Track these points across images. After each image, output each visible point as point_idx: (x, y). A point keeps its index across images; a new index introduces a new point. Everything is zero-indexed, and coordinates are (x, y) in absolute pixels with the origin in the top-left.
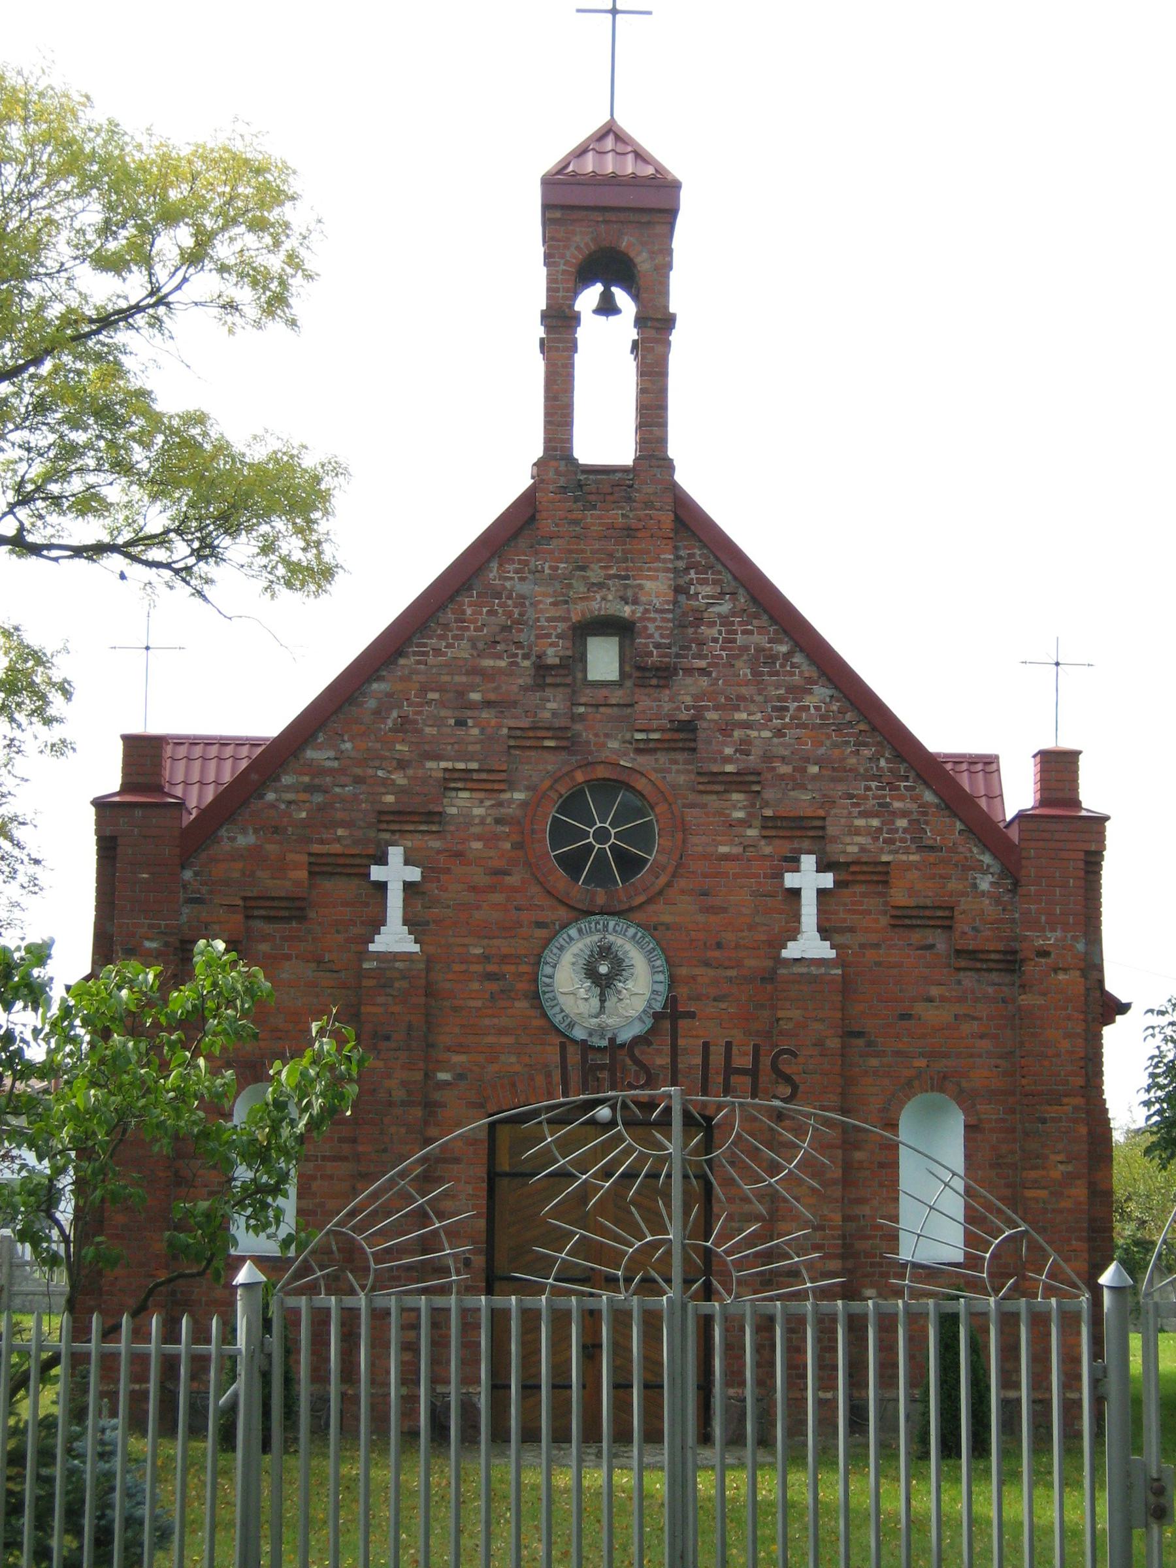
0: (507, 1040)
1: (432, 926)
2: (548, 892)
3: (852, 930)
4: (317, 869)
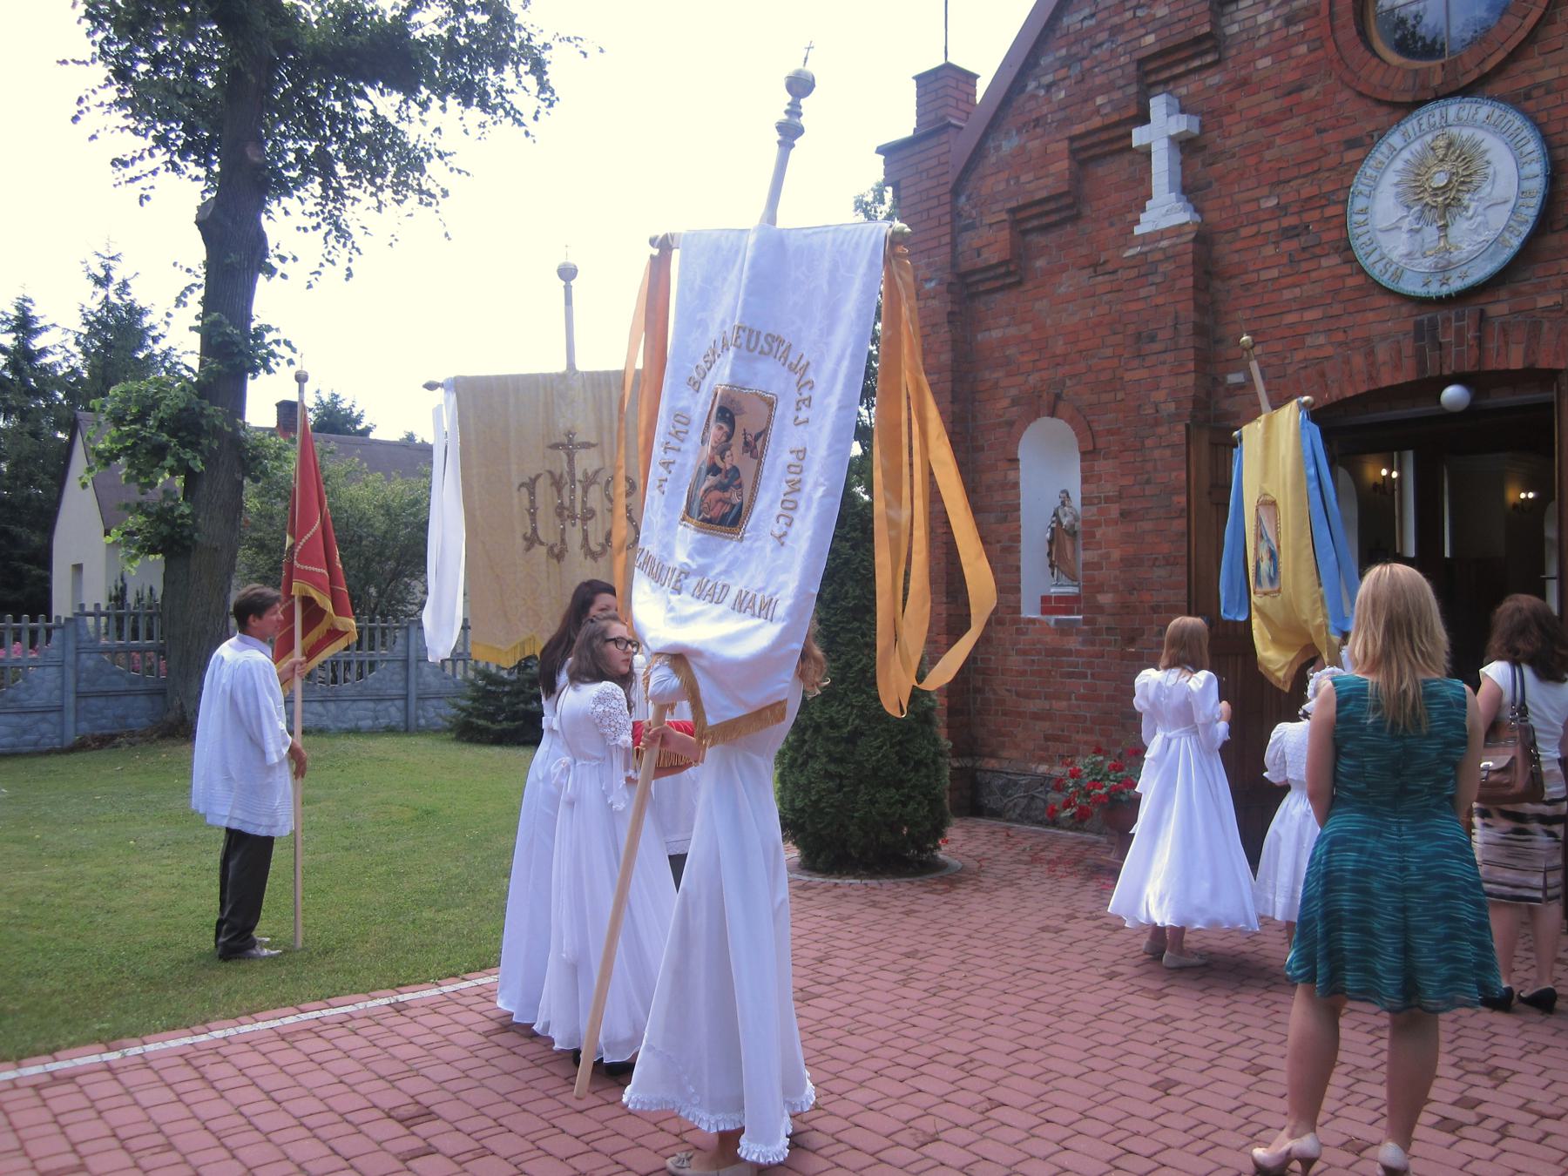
0: (1309, 315)
1: (1215, 186)
2: (1361, 94)
4: (1084, 155)
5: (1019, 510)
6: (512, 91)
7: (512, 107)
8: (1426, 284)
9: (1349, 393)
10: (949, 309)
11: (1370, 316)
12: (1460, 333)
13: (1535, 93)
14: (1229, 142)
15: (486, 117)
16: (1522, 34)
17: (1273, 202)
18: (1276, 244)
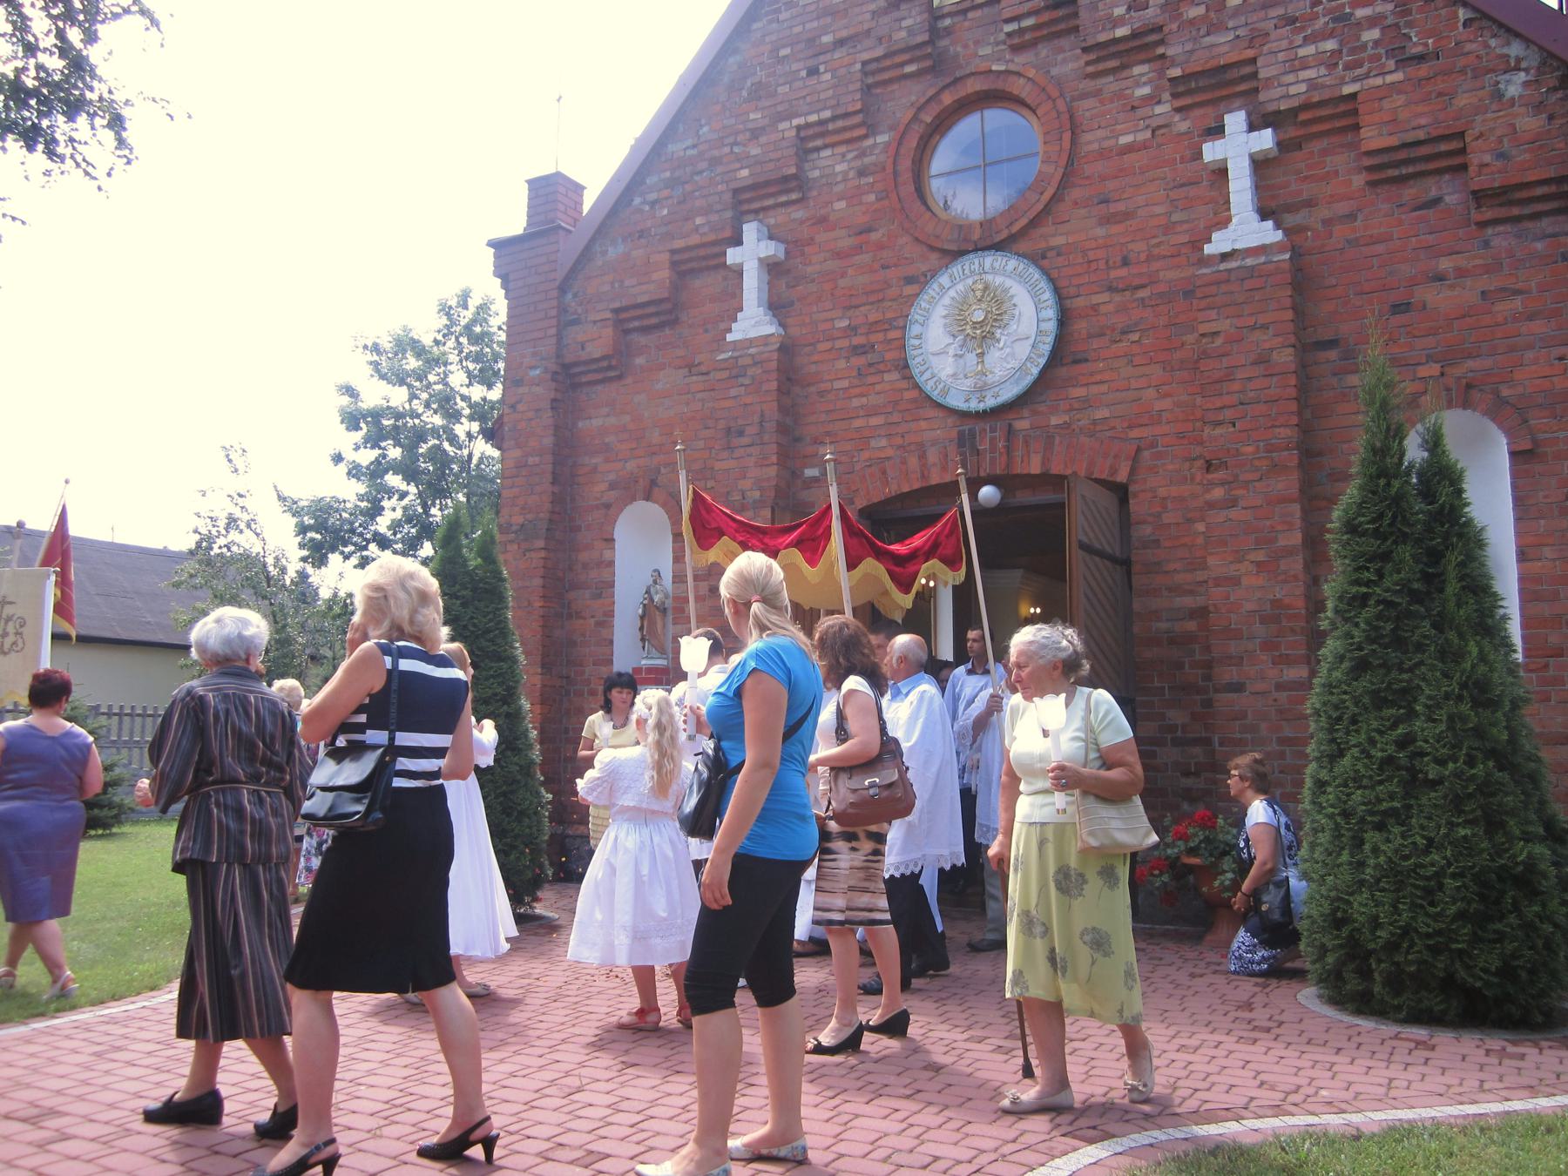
0: (874, 421)
2: (917, 239)
3: (1310, 203)
4: (683, 268)
5: (613, 586)
6: (86, 143)
7: (84, 160)
8: (967, 401)
9: (906, 489)
10: (552, 395)
11: (923, 424)
12: (993, 440)
13: (1049, 255)
14: (809, 269)
15: (49, 165)
16: (1040, 206)
17: (845, 323)
18: (847, 359)
